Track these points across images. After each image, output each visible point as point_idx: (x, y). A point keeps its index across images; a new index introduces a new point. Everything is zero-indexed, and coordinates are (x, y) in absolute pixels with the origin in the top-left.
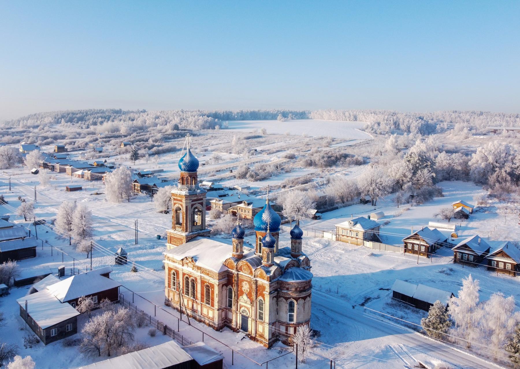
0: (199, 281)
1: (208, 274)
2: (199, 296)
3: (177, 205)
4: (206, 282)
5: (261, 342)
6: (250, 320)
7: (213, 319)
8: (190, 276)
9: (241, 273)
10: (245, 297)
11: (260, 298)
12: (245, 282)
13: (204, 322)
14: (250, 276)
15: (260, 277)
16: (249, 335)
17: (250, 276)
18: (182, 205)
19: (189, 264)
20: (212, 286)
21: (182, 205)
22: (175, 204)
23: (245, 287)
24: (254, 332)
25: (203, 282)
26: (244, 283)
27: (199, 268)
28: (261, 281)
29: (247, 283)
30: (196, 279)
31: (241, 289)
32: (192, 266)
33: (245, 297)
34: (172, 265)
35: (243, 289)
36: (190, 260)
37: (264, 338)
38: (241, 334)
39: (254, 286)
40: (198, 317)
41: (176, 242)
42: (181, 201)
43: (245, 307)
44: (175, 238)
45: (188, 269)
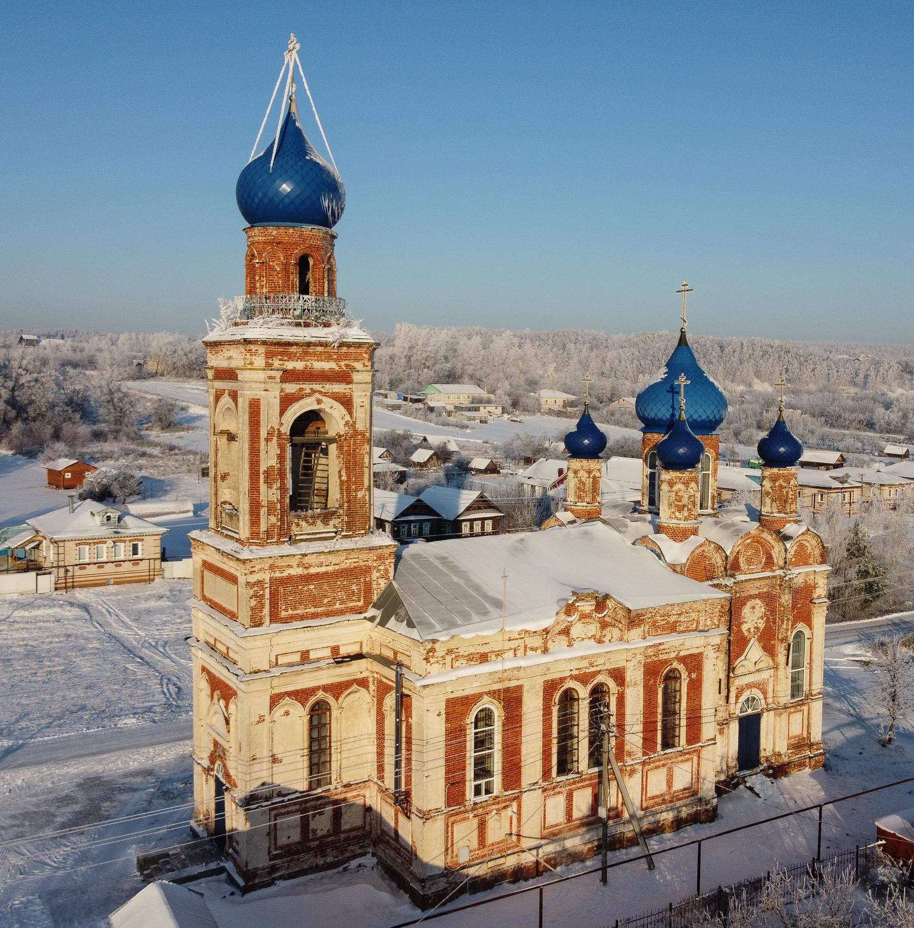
0: (635, 675)
1: (673, 628)
2: (634, 739)
3: (296, 411)
4: (666, 662)
5: (801, 765)
6: (767, 722)
7: (692, 792)
8: (583, 679)
9: (741, 577)
10: (754, 652)
11: (801, 626)
12: (749, 604)
13: (657, 830)
14: (768, 574)
15: (796, 565)
16: (770, 767)
17: (771, 574)
18: (347, 402)
19: (575, 631)
20: (694, 662)
21: (347, 402)
22: (287, 401)
23: (753, 617)
24: (782, 747)
25: (651, 670)
26: (746, 611)
27: (633, 619)
28: (799, 574)
29: (758, 601)
30: (618, 675)
31: (740, 631)
32: (593, 628)
33: (754, 652)
34: (470, 679)
35: (744, 628)
36: (587, 607)
37: (811, 746)
38: (756, 780)
39: (786, 599)
40: (628, 830)
41: (315, 601)
42: (344, 377)
43: (749, 686)
44: (308, 579)
45: (582, 652)
